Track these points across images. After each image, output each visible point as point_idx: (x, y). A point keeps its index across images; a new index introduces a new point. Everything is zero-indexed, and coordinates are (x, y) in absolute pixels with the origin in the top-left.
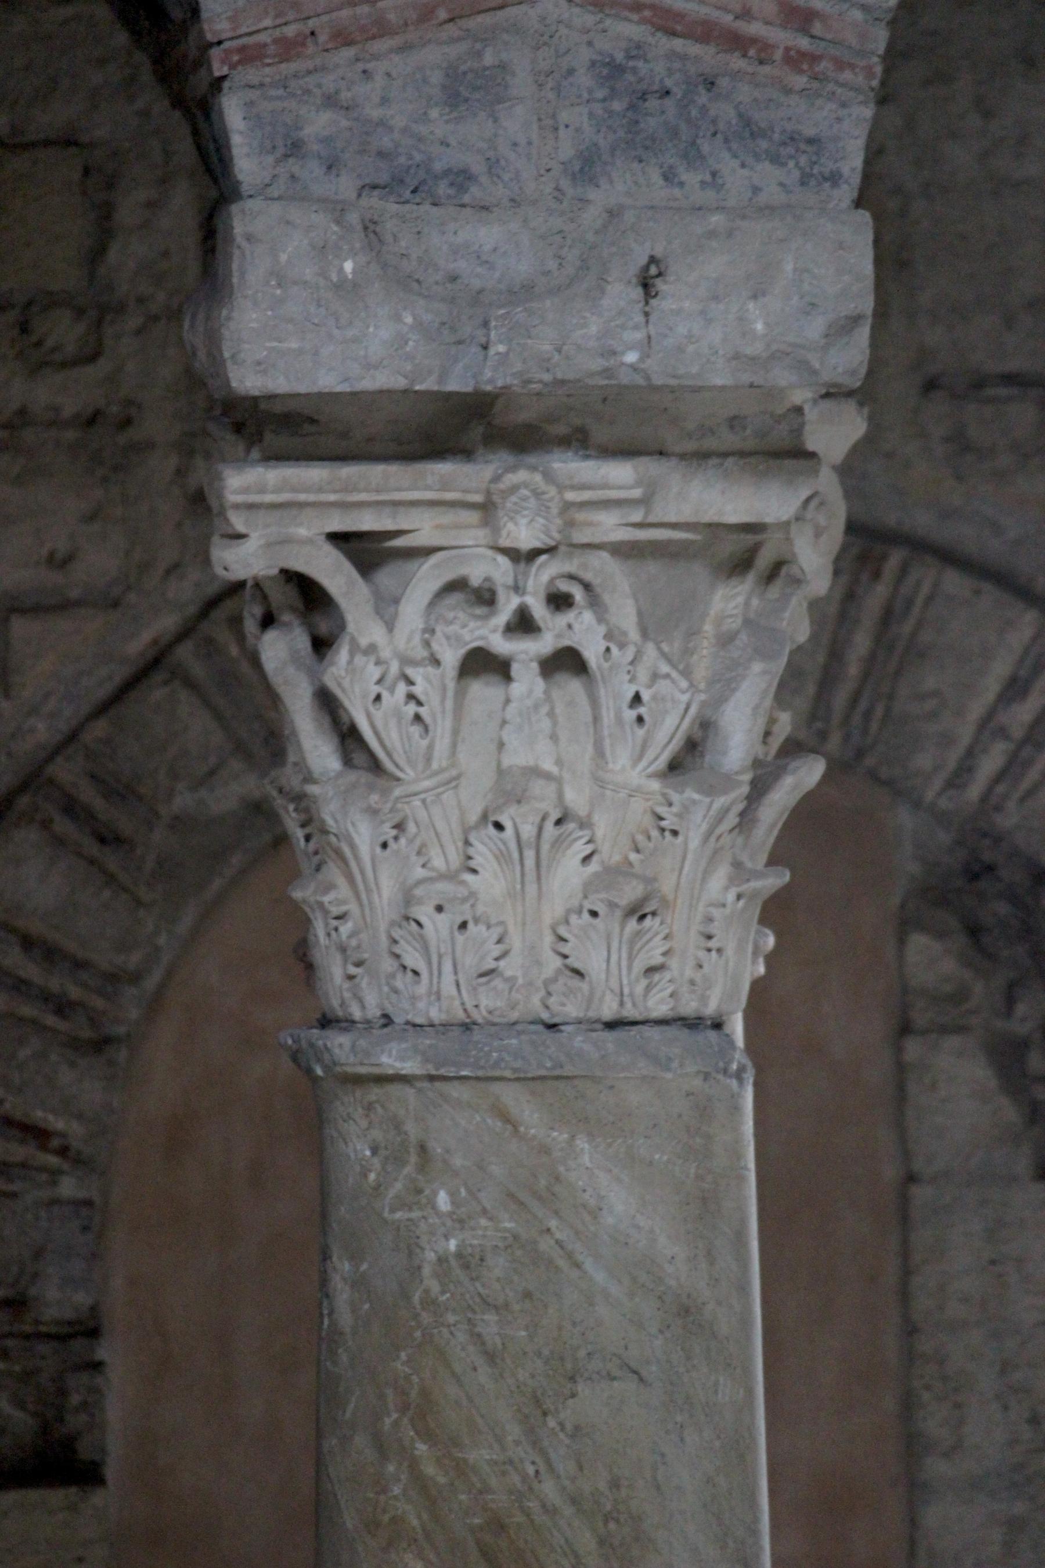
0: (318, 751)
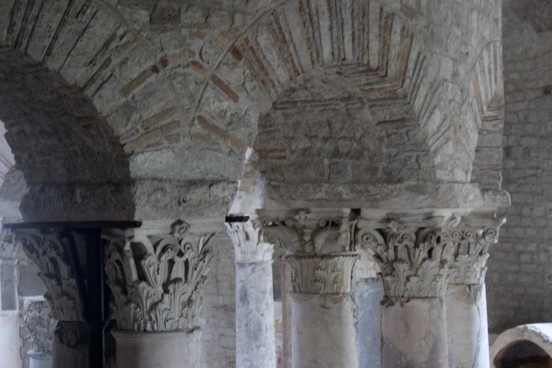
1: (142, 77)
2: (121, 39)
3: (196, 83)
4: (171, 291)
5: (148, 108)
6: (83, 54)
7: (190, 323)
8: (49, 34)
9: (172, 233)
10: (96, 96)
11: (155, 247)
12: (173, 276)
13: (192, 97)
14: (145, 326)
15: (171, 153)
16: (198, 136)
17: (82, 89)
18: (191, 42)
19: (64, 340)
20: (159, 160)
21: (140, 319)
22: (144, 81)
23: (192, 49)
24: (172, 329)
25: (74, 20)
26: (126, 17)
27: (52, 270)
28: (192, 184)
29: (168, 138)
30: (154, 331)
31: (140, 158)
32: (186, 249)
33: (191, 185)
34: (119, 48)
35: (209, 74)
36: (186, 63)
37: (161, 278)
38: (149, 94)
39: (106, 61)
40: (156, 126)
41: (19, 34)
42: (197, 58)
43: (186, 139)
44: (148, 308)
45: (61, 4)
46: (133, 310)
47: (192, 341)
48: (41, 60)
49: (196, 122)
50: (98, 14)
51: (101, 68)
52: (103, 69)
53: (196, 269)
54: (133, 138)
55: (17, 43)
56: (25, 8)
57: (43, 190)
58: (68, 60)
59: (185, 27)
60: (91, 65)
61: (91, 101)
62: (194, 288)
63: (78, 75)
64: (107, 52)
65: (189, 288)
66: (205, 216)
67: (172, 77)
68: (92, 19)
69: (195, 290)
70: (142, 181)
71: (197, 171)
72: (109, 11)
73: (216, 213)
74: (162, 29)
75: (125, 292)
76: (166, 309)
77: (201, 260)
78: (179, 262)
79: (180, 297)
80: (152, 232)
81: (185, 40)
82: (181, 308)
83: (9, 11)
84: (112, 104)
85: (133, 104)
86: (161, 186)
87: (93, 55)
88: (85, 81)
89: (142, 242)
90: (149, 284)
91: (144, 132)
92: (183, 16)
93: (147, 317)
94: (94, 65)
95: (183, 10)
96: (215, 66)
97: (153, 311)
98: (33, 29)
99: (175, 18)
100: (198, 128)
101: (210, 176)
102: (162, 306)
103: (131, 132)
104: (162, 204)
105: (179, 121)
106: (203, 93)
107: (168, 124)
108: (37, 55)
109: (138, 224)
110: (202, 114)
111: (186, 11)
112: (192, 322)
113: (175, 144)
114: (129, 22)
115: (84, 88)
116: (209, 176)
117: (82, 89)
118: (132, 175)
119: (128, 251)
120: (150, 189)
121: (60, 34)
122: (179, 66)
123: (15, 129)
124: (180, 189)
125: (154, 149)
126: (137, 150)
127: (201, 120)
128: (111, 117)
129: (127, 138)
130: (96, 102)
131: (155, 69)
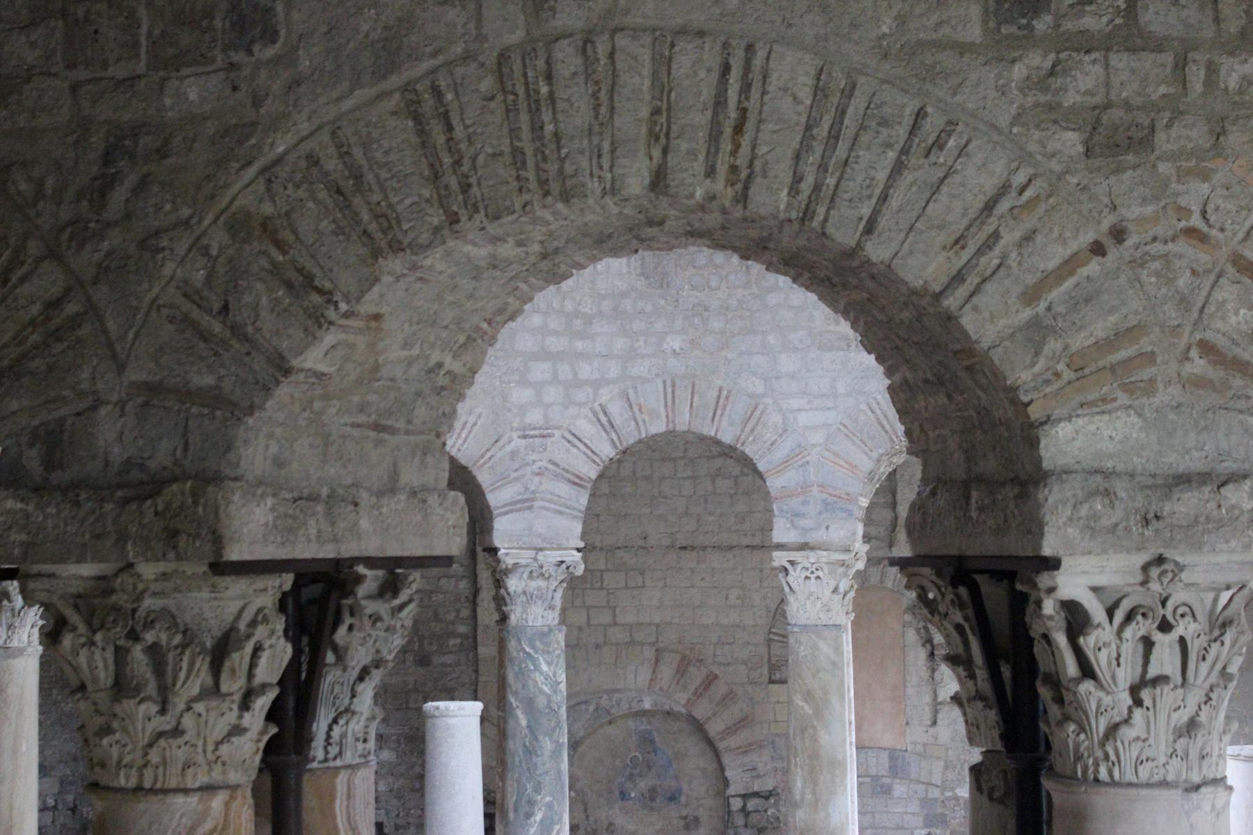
0: (787, 589)
1: (1070, 265)
2: (1021, 193)
3: (1194, 272)
4: (1147, 702)
5: (1081, 328)
6: (940, 228)
7: (1196, 769)
8: (868, 192)
9: (1144, 583)
10: (968, 307)
11: (1110, 613)
12: (1153, 672)
13: (1184, 302)
14: (1097, 771)
15: (1134, 419)
16: (1198, 383)
17: (938, 296)
18: (1181, 188)
19: (984, 786)
20: (1106, 433)
21: (1086, 754)
22: (1072, 273)
23: (1183, 205)
24: (1152, 781)
25: (922, 161)
26: (1032, 147)
27: (960, 650)
28: (1183, 480)
29: (1128, 389)
30: (1114, 784)
31: (1063, 430)
32: (1178, 617)
33: (1177, 485)
34: (1016, 211)
35: (1225, 252)
36: (1170, 233)
37: (1126, 675)
38: (1085, 299)
39: (990, 236)
40: (1101, 363)
41: (810, 197)
42: (1196, 221)
43: (1169, 390)
44: (1101, 734)
45: (894, 133)
46: (1072, 736)
47: (1199, 807)
48: (853, 244)
49: (1194, 353)
50: (970, 147)
51: (980, 252)
52: (983, 255)
53: (1204, 659)
54: (1048, 390)
55: (807, 214)
56: (823, 147)
57: (933, 493)
58: (908, 241)
59: (1167, 160)
60: (957, 247)
61: (956, 318)
62: (1205, 699)
63: (930, 269)
64: (991, 219)
65: (1195, 697)
66: (1205, 549)
67: (1138, 263)
68: (959, 156)
69: (1206, 703)
70: (1064, 476)
71: (1195, 454)
72: (996, 138)
73: (1233, 544)
74: (1113, 166)
75: (1060, 700)
76: (1138, 738)
77: (1215, 640)
78: (1165, 645)
79: (1169, 716)
80: (1101, 580)
81: (1167, 186)
82: (1171, 738)
83: (790, 154)
84: (1003, 322)
85: (1048, 321)
86: (1107, 485)
87: (962, 227)
88: (945, 279)
89: (1077, 599)
90: (1100, 686)
91: (1073, 376)
92: (1161, 137)
93: (1099, 754)
94: (963, 248)
95: (1160, 125)
96: (1241, 235)
97: (1111, 741)
98: (837, 186)
99: (1142, 142)
100: (1199, 365)
101: (1228, 466)
102: (1127, 733)
103: (1045, 377)
104: (1106, 522)
105: (1153, 353)
106: (1209, 294)
107: (1130, 360)
108: (844, 234)
109: (1053, 564)
110: (1209, 336)
111: (1168, 126)
112: (1200, 767)
113: (1145, 400)
114: (1039, 157)
115: (942, 293)
116: (1225, 464)
117: (938, 296)
118: (1046, 465)
119: (1050, 618)
120: (1079, 492)
121: (891, 191)
122: (1155, 239)
123: (898, 377)
124: (1149, 492)
125: (1097, 410)
126: (1057, 413)
127: (1207, 348)
128: (1000, 349)
129: (1035, 388)
130: (968, 321)
131: (1098, 249)
